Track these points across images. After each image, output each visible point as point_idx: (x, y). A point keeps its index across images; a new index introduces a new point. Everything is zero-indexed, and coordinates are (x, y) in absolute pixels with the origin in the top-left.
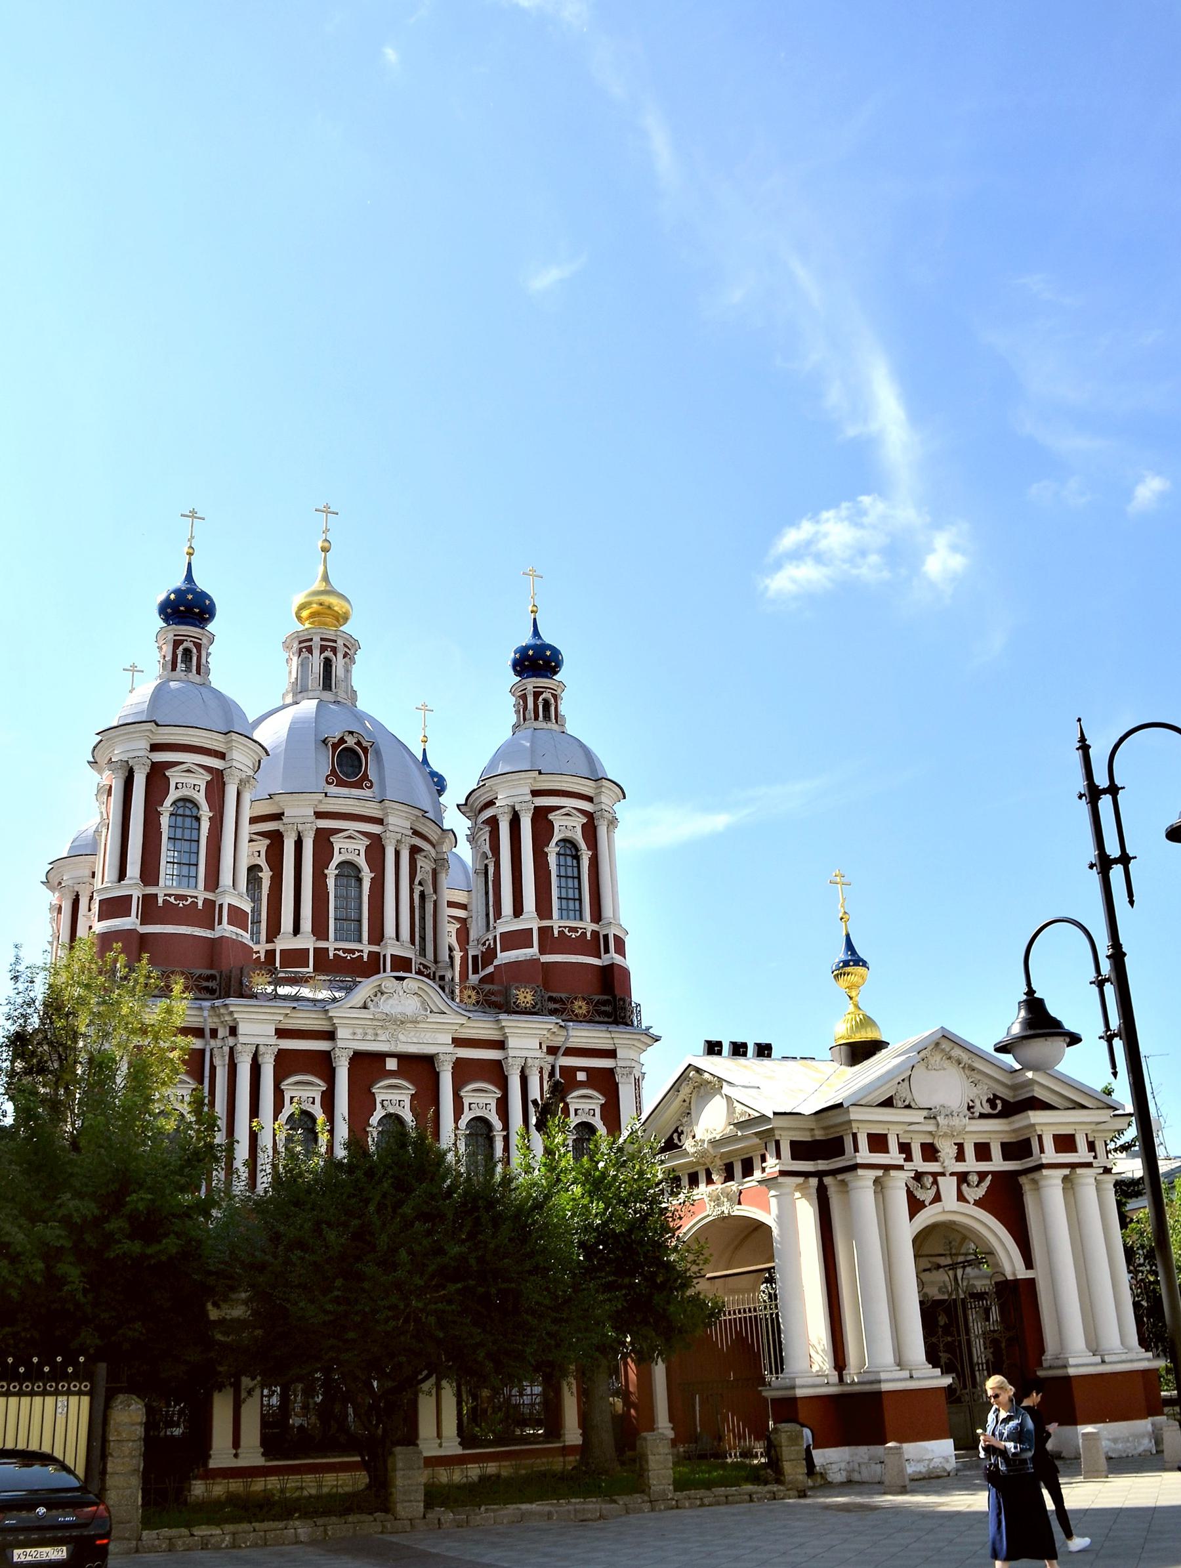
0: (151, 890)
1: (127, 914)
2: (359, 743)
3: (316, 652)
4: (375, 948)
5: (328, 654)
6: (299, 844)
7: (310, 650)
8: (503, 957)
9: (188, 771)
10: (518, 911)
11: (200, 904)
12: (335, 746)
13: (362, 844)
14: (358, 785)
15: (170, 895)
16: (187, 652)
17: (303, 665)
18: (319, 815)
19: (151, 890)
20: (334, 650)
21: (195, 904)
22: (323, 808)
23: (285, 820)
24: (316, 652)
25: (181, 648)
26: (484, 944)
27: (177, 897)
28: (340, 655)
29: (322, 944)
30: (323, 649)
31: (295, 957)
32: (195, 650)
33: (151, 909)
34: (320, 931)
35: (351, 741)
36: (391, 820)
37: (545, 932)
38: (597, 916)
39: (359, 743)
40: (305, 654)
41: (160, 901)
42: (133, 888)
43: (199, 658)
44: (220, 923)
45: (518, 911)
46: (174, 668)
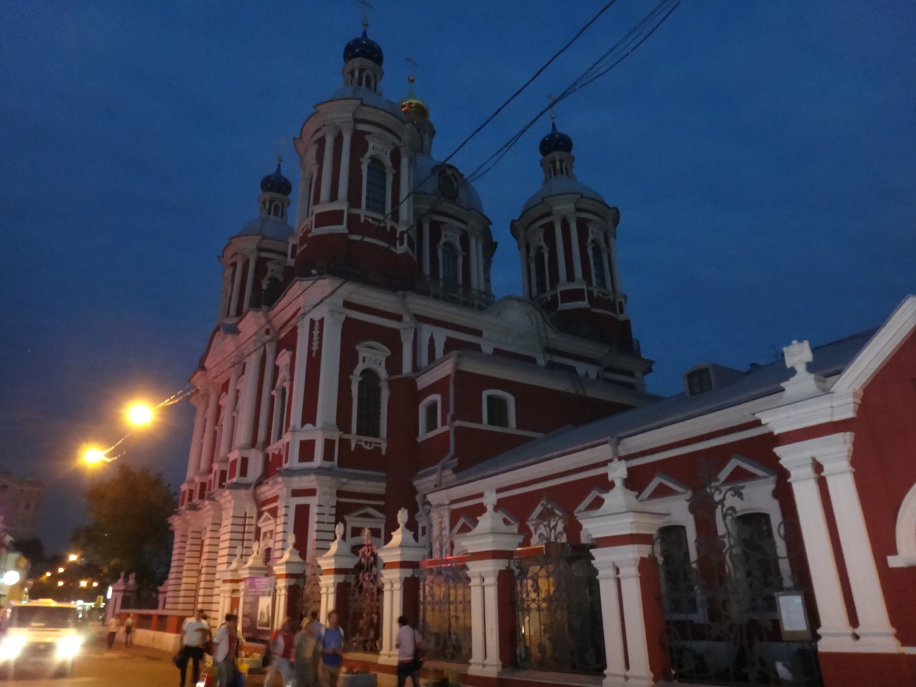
0: (355, 211)
1: (342, 223)
2: (453, 175)
8: (563, 306)
10: (571, 277)
11: (388, 228)
15: (369, 217)
19: (355, 211)
21: (385, 227)
25: (365, 73)
27: (373, 219)
33: (354, 223)
37: (590, 293)
38: (614, 291)
39: (453, 175)
41: (362, 219)
42: (341, 205)
45: (571, 277)
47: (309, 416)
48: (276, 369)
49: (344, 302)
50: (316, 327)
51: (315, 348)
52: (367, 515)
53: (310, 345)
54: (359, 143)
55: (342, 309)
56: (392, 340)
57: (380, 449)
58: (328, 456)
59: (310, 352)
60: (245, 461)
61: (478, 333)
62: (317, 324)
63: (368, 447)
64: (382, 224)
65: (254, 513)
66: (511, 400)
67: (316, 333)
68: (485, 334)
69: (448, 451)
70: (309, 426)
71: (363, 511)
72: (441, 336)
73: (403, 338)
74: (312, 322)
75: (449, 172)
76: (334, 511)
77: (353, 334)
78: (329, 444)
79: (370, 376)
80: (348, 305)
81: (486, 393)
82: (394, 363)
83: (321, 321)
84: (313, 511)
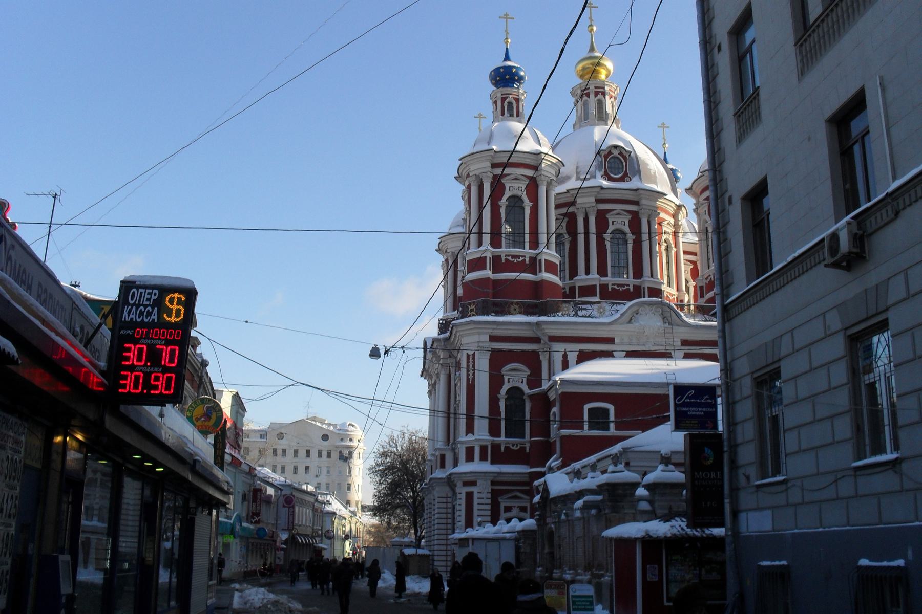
2: (621, 154)
3: (592, 96)
4: (637, 282)
5: (600, 96)
6: (586, 221)
7: (588, 95)
9: (516, 179)
12: (606, 157)
13: (626, 219)
14: (622, 180)
16: (510, 104)
17: (586, 105)
18: (598, 201)
20: (604, 94)
22: (600, 197)
23: (577, 206)
24: (592, 96)
26: (707, 278)
28: (607, 97)
29: (604, 280)
30: (596, 94)
31: (588, 291)
32: (514, 103)
34: (602, 271)
35: (616, 153)
36: (644, 202)
39: (621, 154)
40: (585, 98)
41: (503, 261)
43: (518, 108)
44: (540, 271)
46: (503, 114)
47: (470, 429)
48: (456, 385)
49: (490, 336)
50: (471, 359)
51: (471, 377)
52: (516, 497)
53: (468, 375)
54: (498, 187)
55: (488, 344)
56: (532, 361)
57: (525, 448)
58: (483, 458)
59: (468, 380)
60: (443, 457)
61: (611, 341)
62: (471, 357)
63: (515, 448)
64: (521, 259)
65: (450, 495)
66: (612, 408)
67: (471, 364)
68: (616, 341)
69: (555, 453)
70: (470, 435)
71: (514, 494)
72: (574, 349)
73: (542, 358)
74: (468, 356)
75: (616, 153)
76: (489, 496)
77: (498, 360)
78: (483, 449)
79: (515, 392)
80: (493, 339)
81: (586, 407)
82: (535, 380)
83: (474, 355)
84: (476, 496)
